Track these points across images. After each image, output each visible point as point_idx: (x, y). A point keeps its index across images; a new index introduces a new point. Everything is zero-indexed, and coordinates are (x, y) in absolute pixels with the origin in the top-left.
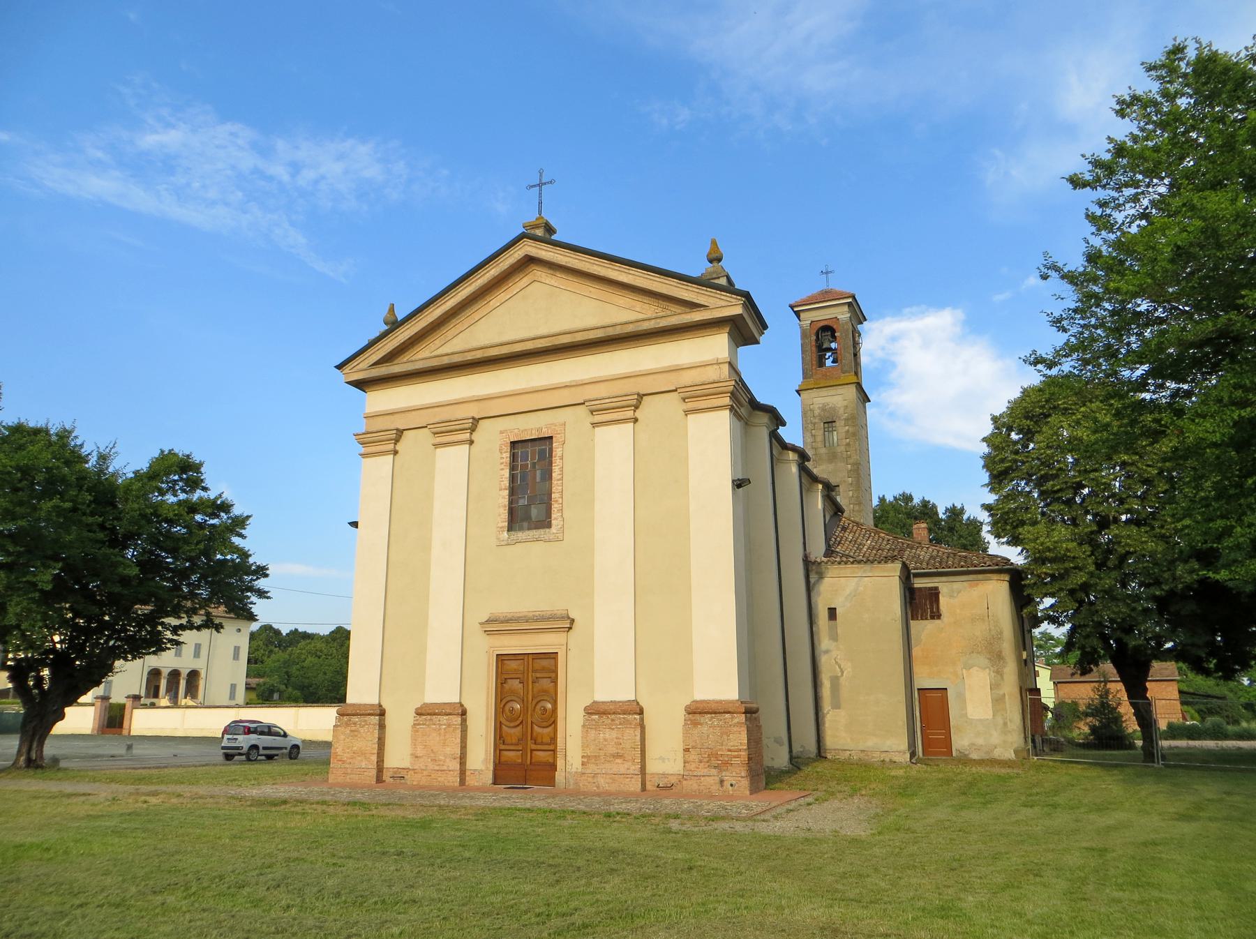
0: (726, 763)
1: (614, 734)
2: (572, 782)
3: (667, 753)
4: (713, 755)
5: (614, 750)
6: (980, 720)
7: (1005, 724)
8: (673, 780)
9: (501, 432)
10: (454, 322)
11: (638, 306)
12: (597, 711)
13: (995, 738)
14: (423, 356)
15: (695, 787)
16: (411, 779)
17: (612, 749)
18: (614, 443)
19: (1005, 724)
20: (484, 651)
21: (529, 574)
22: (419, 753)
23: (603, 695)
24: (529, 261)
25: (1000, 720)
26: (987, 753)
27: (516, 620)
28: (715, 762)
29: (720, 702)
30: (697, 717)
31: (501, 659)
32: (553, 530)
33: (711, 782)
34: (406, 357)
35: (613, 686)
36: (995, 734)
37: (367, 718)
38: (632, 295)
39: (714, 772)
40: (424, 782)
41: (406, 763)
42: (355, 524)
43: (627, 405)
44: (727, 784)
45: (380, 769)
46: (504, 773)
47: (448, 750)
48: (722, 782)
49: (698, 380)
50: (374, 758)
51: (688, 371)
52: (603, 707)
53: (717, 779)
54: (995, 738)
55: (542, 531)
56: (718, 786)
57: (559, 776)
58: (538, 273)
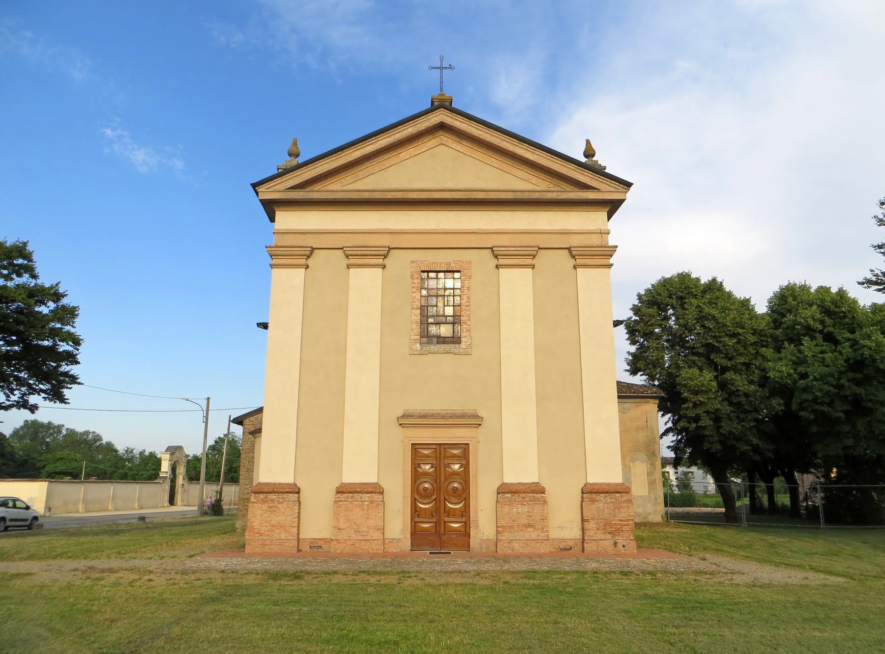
0: (618, 530)
1: (526, 509)
2: (484, 546)
3: (564, 521)
4: (607, 524)
5: (526, 522)
6: (641, 496)
7: (656, 499)
8: (571, 543)
9: (412, 262)
10: (367, 164)
11: (534, 180)
12: (504, 490)
13: (650, 508)
14: (336, 187)
15: (595, 548)
16: (337, 548)
17: (524, 521)
18: (516, 284)
19: (656, 499)
20: (401, 441)
21: (440, 382)
22: (342, 525)
23: (511, 477)
24: (442, 127)
25: (653, 496)
26: (645, 518)
27: (453, 416)
28: (609, 529)
29: (600, 484)
30: (594, 495)
31: (415, 448)
32: (463, 345)
33: (608, 544)
34: (317, 187)
35: (520, 470)
36: (649, 505)
37: (285, 495)
38: (530, 170)
39: (609, 536)
40: (348, 550)
41: (326, 534)
42: (265, 326)
43: (506, 255)
44: (620, 546)
45: (299, 540)
46: (418, 538)
47: (371, 523)
48: (615, 544)
49: (585, 243)
50: (295, 530)
51: (577, 236)
52: (514, 489)
53: (612, 542)
54: (650, 508)
55: (453, 346)
56: (612, 547)
57: (474, 542)
58: (444, 138)
